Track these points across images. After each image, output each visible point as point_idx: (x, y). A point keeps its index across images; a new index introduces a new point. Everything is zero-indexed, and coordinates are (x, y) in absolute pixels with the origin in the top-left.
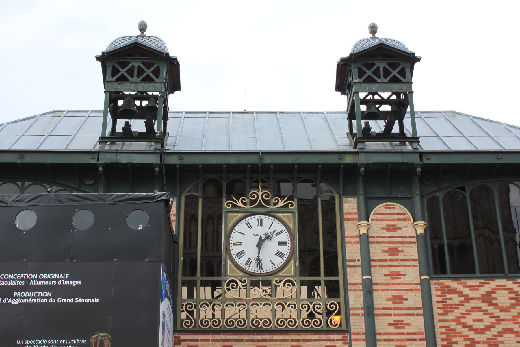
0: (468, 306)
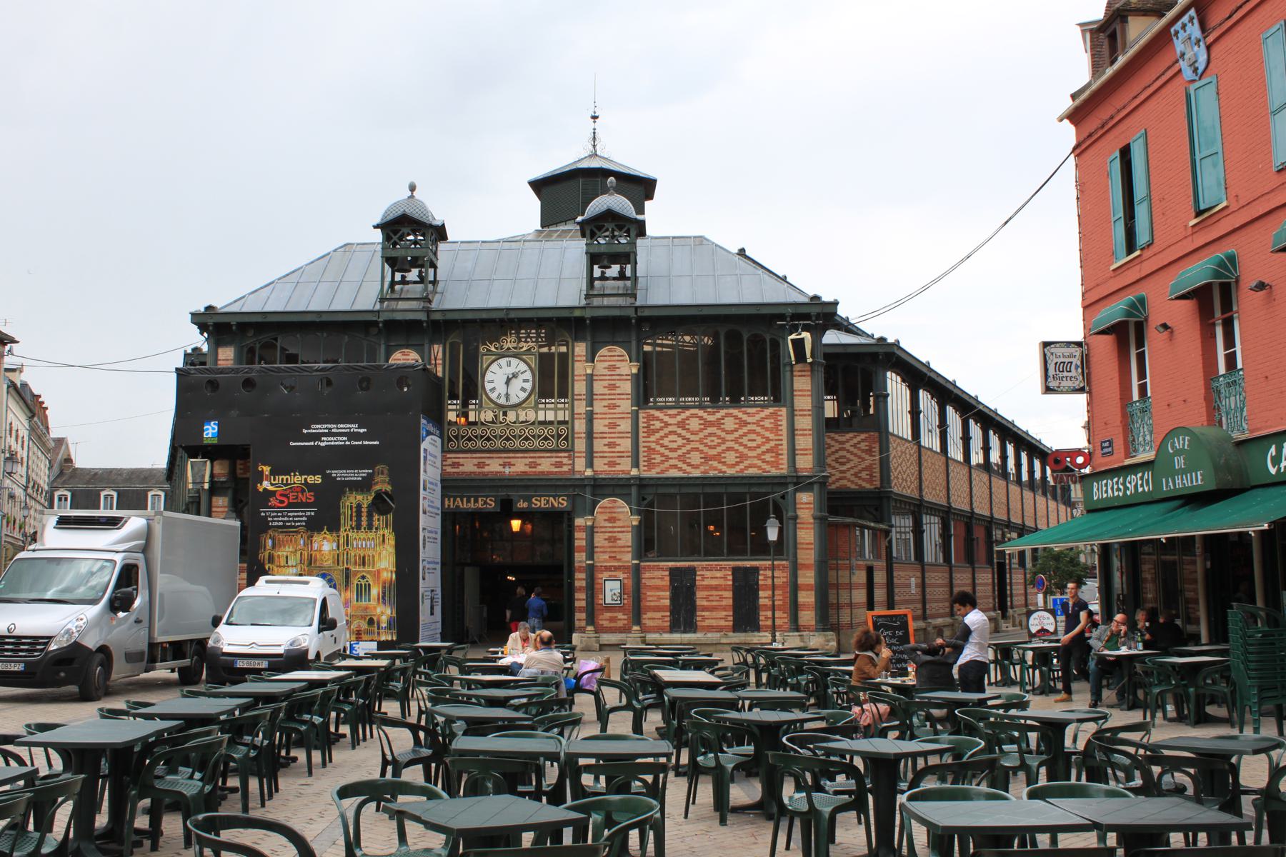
0: (666, 430)
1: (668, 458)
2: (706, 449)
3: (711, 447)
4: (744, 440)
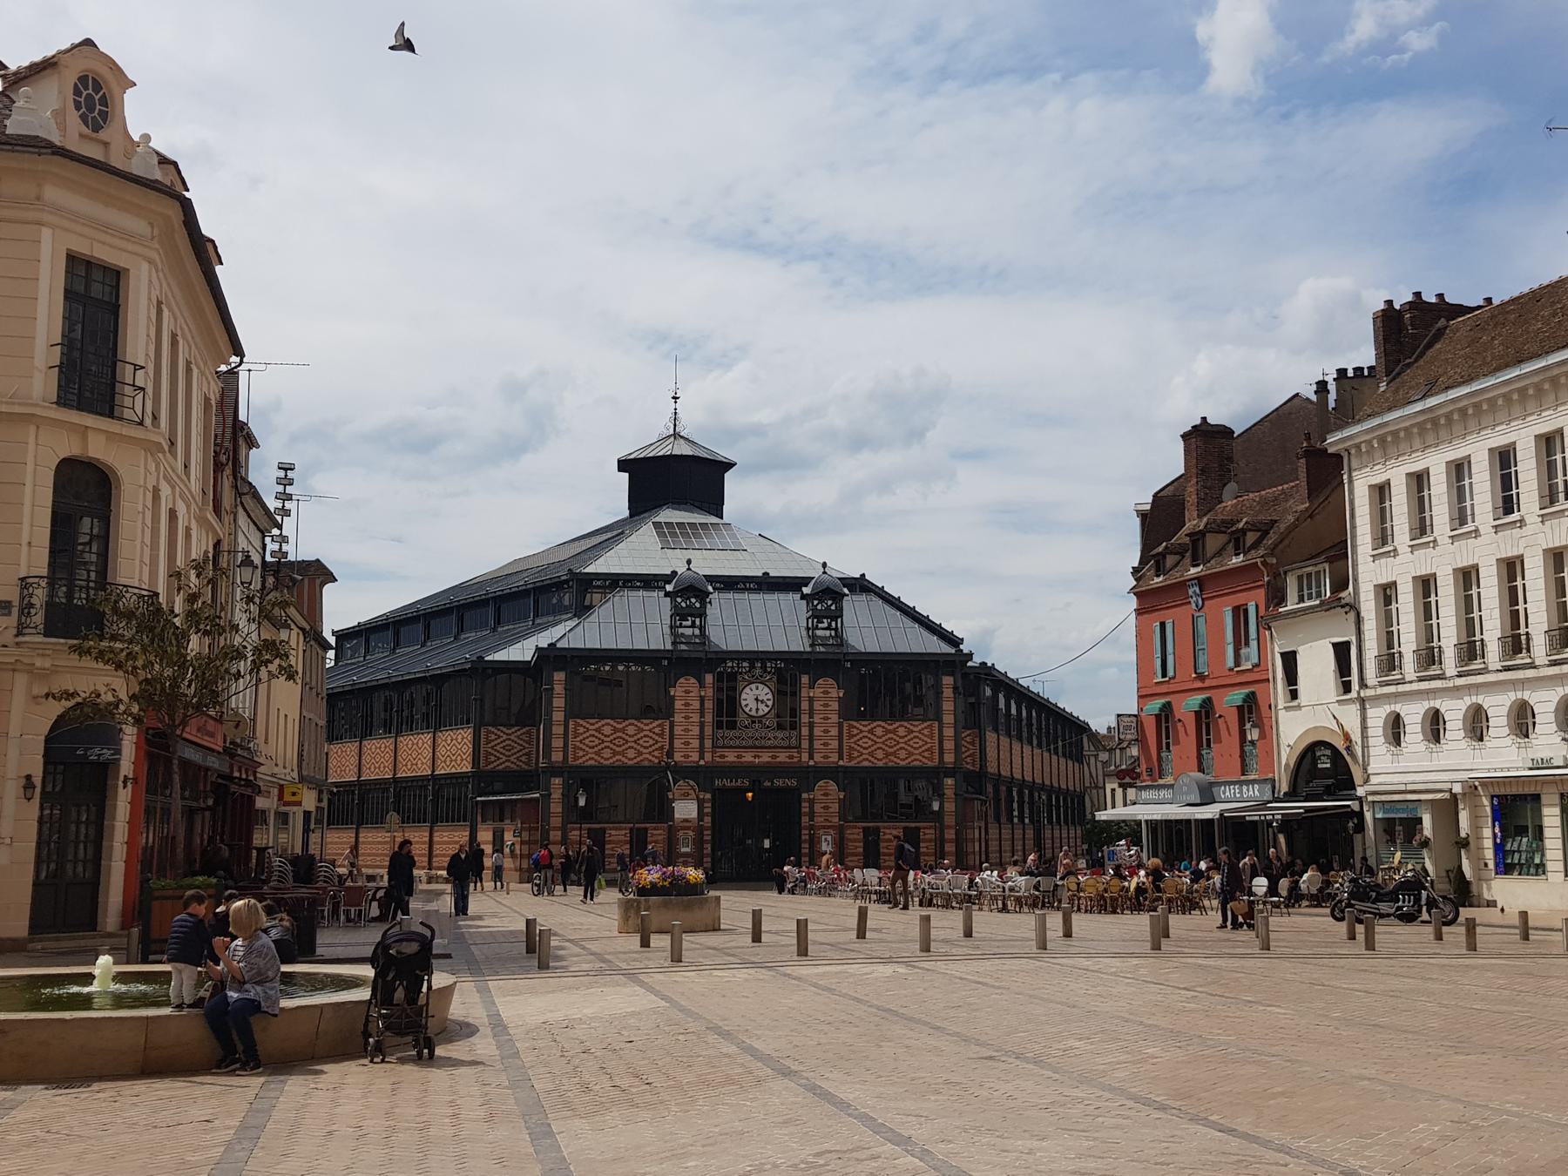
0: (861, 735)
1: (862, 754)
3: (890, 747)
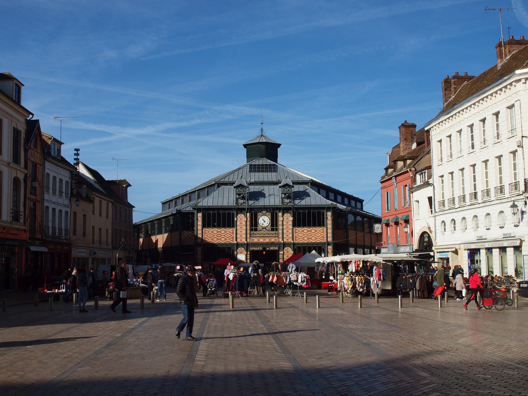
0: (299, 232)
1: (300, 239)
2: (308, 237)
3: (309, 236)
4: (316, 235)
